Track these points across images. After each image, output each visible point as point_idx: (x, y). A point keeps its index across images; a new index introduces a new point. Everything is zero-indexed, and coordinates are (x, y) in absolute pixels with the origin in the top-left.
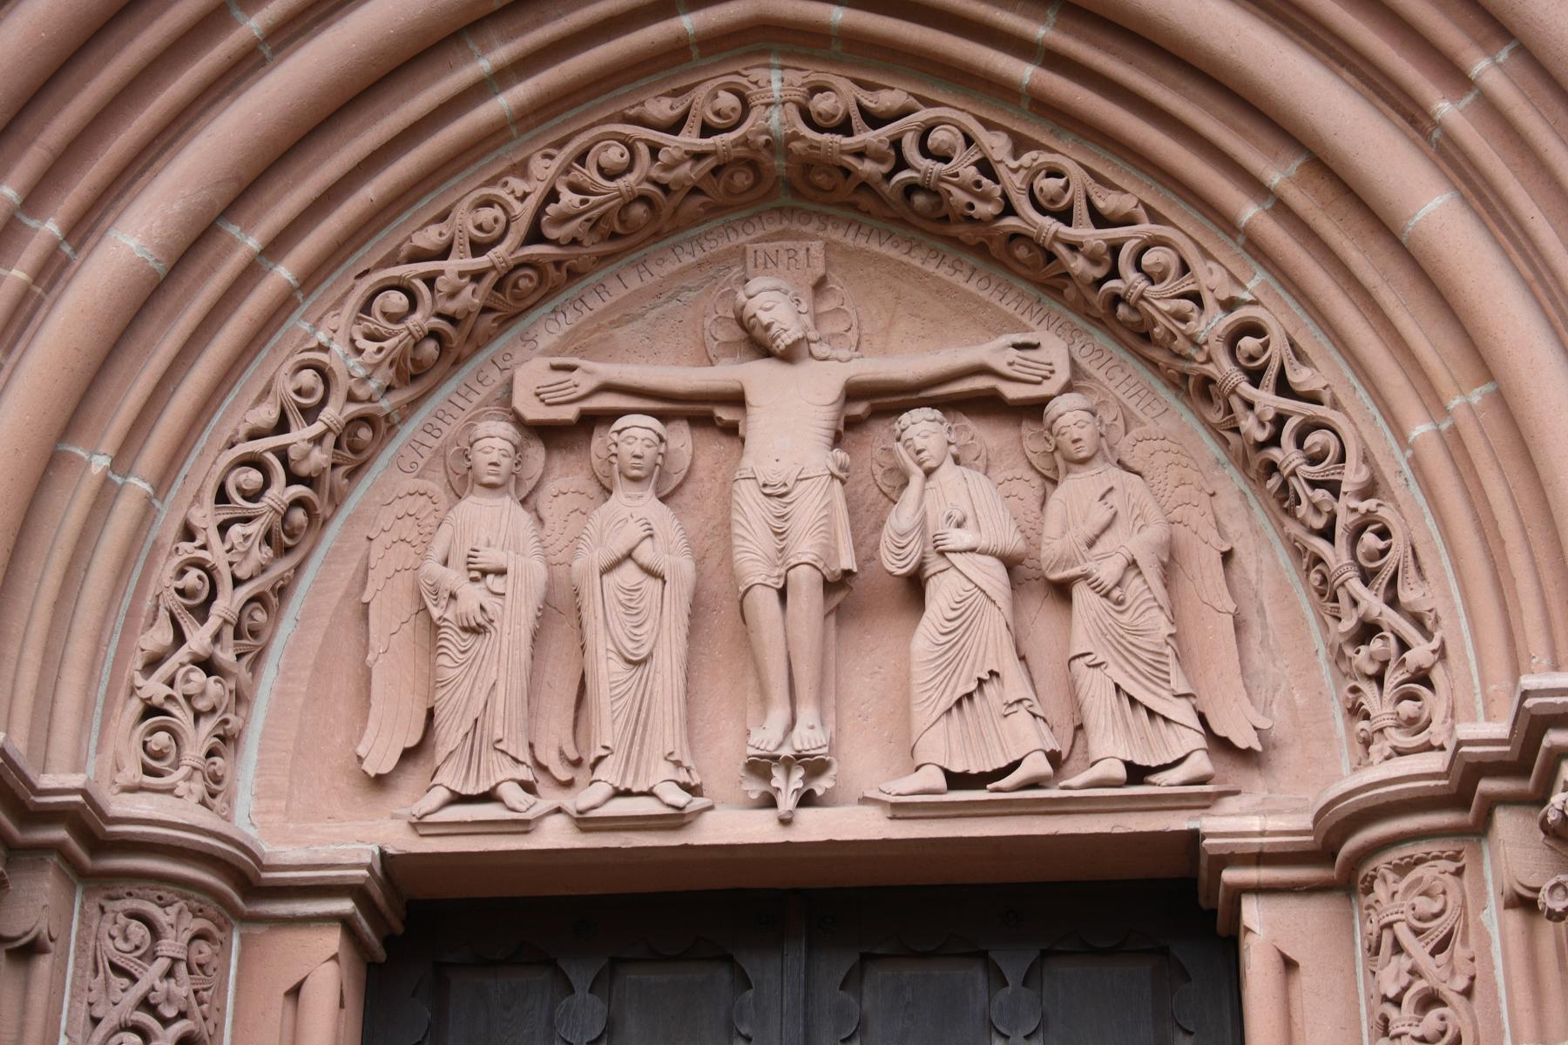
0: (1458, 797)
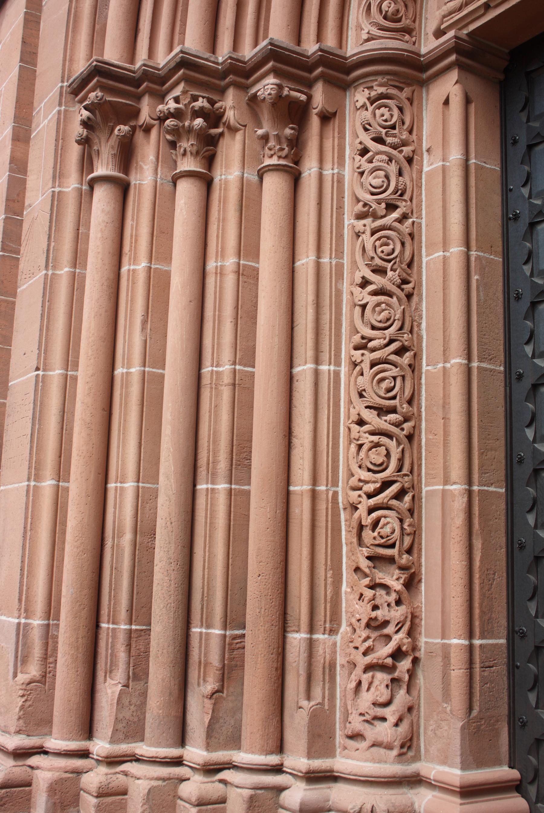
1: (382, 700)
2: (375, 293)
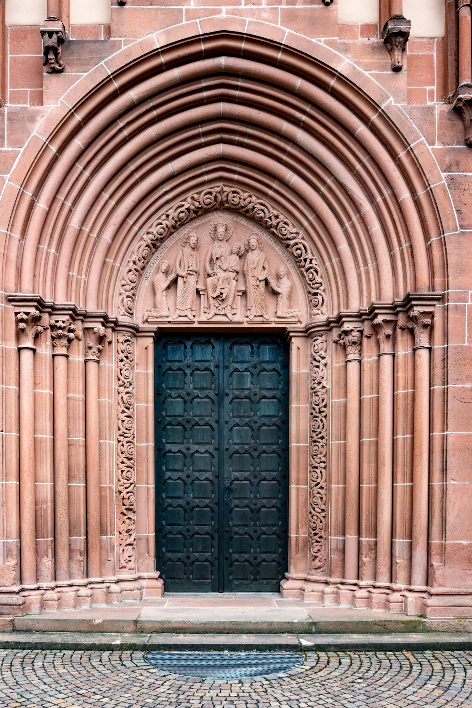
2: (127, 416)
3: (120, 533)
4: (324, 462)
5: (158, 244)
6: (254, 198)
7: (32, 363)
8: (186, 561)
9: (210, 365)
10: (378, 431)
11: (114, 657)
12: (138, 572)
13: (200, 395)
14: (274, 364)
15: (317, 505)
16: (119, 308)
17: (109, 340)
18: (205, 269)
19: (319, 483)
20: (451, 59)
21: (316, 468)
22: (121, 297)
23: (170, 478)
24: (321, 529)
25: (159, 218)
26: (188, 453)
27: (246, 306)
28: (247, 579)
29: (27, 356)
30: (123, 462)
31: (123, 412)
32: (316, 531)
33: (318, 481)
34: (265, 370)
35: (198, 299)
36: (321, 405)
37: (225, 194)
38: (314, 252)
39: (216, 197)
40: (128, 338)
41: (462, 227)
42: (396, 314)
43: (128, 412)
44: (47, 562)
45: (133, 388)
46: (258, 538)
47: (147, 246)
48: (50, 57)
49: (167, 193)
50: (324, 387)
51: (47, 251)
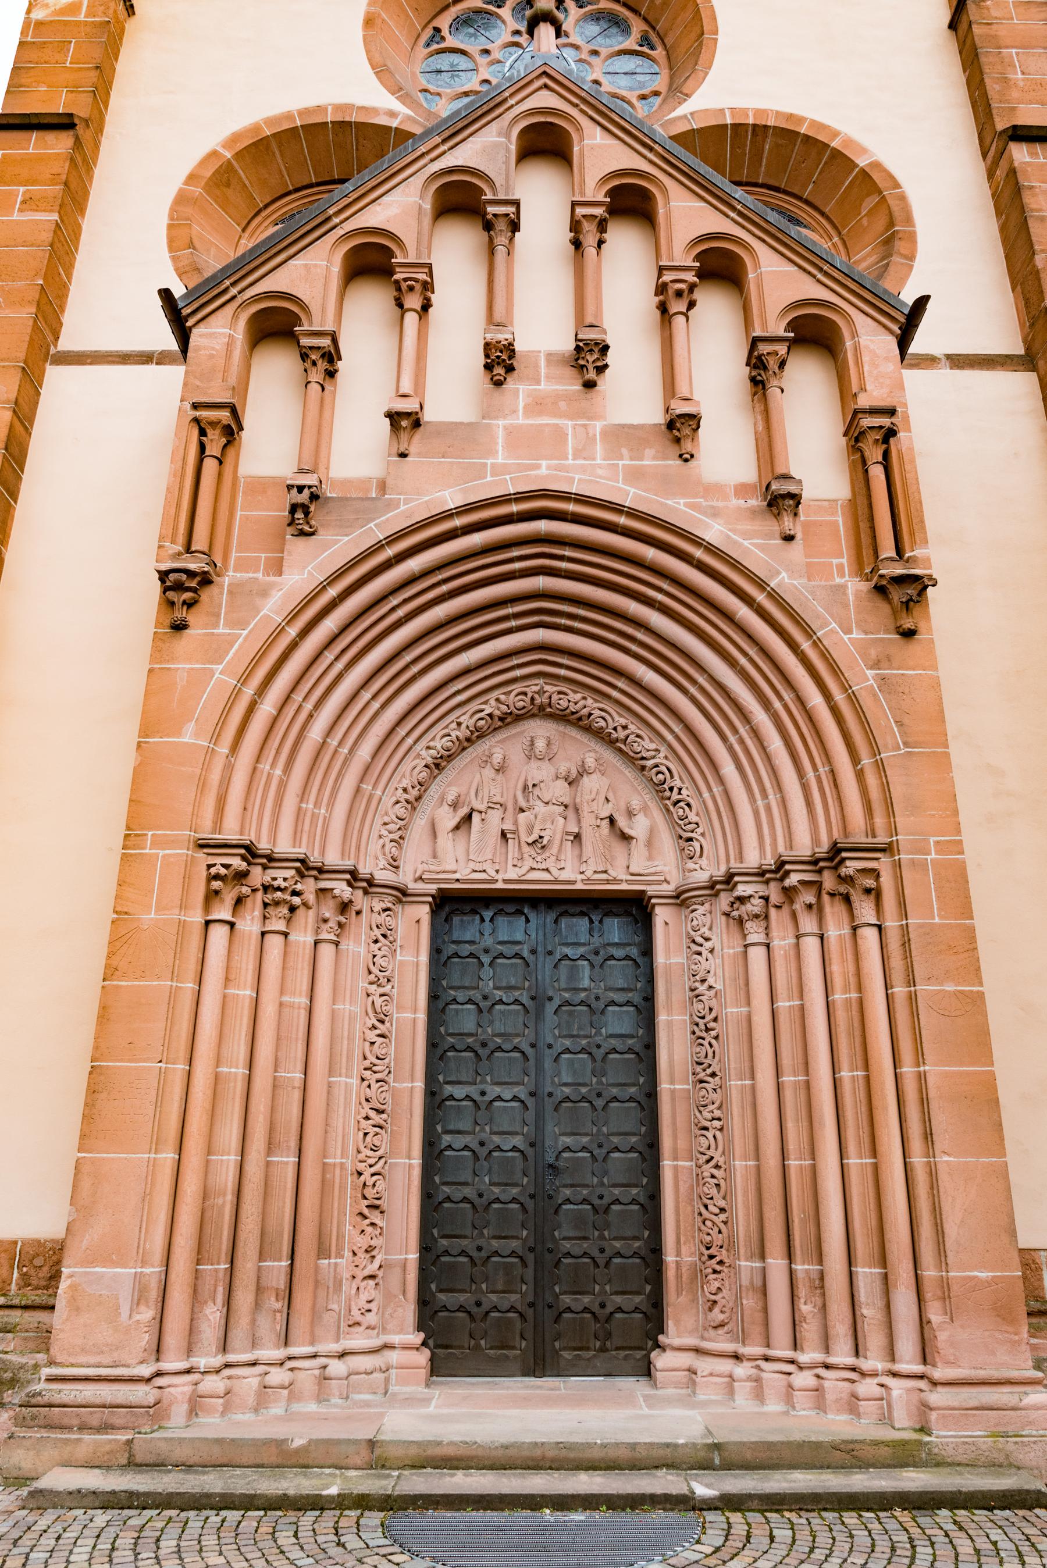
0: (712, 887)
1: (370, 1299)
3: (355, 1254)
4: (719, 1119)
5: (443, 764)
6: (590, 701)
7: (227, 945)
8: (474, 1310)
9: (521, 949)
10: (806, 1063)
11: (324, 1524)
12: (383, 1334)
13: (504, 999)
14: (628, 949)
15: (712, 1198)
16: (377, 858)
17: (357, 908)
18: (516, 801)
19: (712, 1158)
20: (864, 526)
21: (706, 1129)
22: (381, 841)
23: (450, 1146)
24: (721, 1247)
25: (446, 727)
26: (482, 1101)
27: (580, 856)
28: (588, 1349)
29: (219, 934)
30: (367, 1118)
31: (374, 1027)
32: (712, 1251)
33: (711, 1153)
34: (612, 957)
35: (504, 845)
36: (708, 1018)
37: (547, 694)
38: (684, 777)
39: (532, 699)
40: (390, 905)
41: (906, 744)
42: (820, 871)
43: (382, 1029)
44: (213, 1314)
45: (393, 987)
46: (607, 1264)
47: (426, 766)
48: (296, 516)
49: (458, 692)
50: (711, 987)
51: (269, 773)
